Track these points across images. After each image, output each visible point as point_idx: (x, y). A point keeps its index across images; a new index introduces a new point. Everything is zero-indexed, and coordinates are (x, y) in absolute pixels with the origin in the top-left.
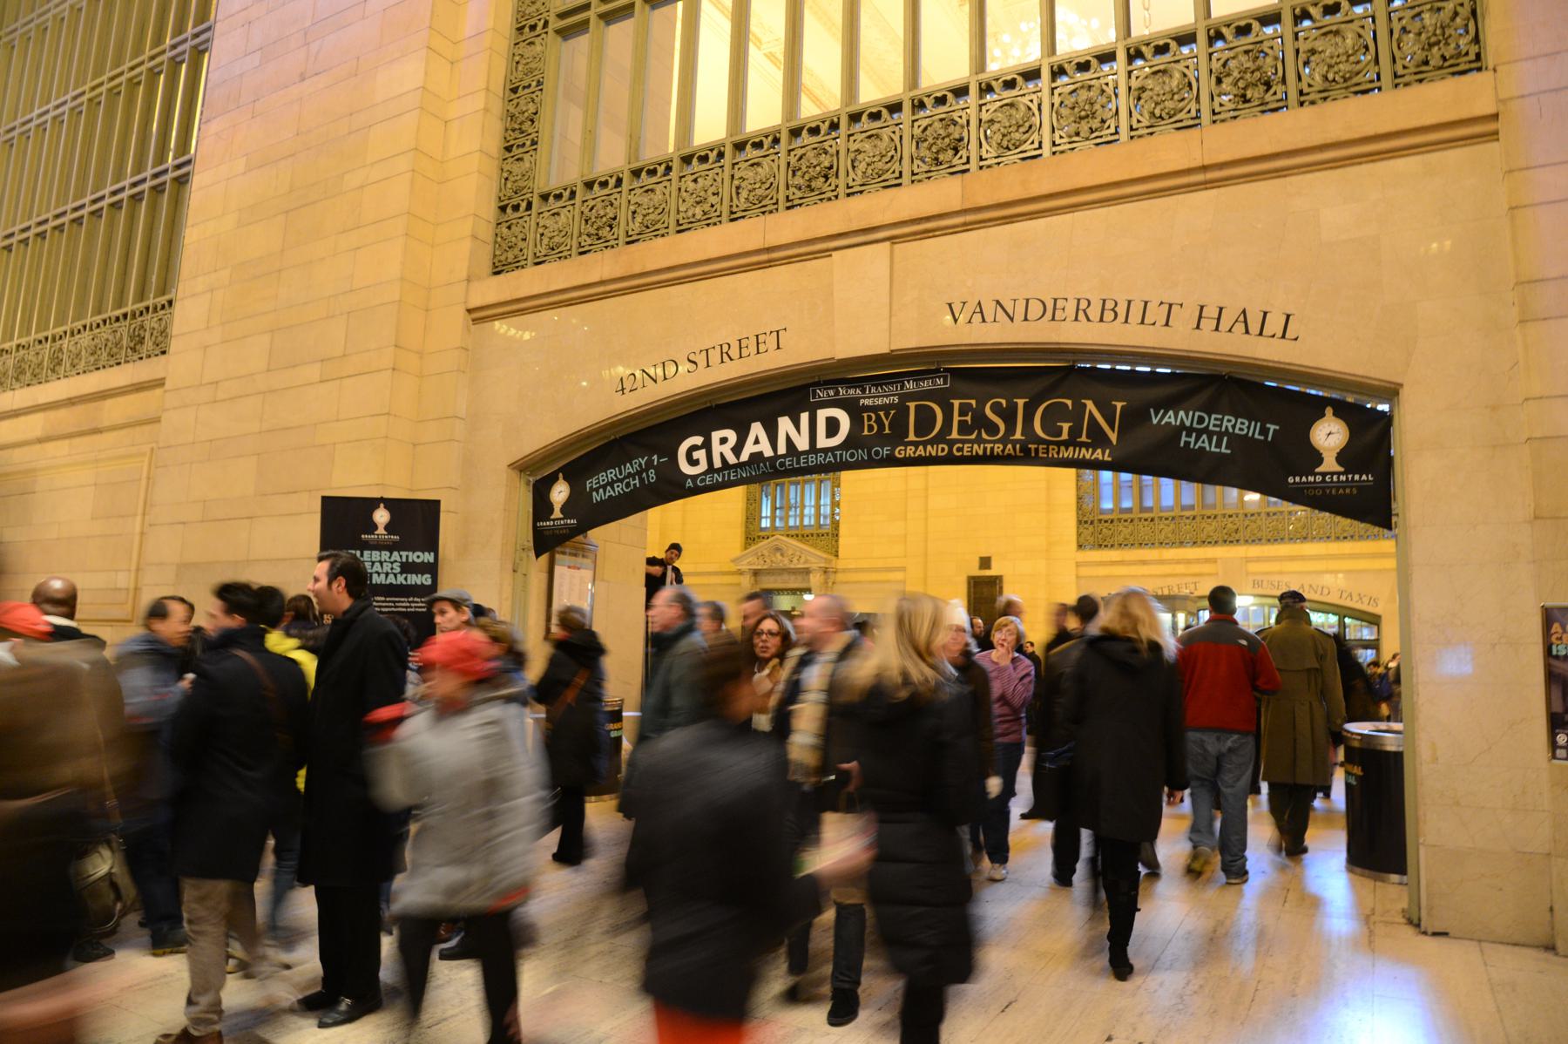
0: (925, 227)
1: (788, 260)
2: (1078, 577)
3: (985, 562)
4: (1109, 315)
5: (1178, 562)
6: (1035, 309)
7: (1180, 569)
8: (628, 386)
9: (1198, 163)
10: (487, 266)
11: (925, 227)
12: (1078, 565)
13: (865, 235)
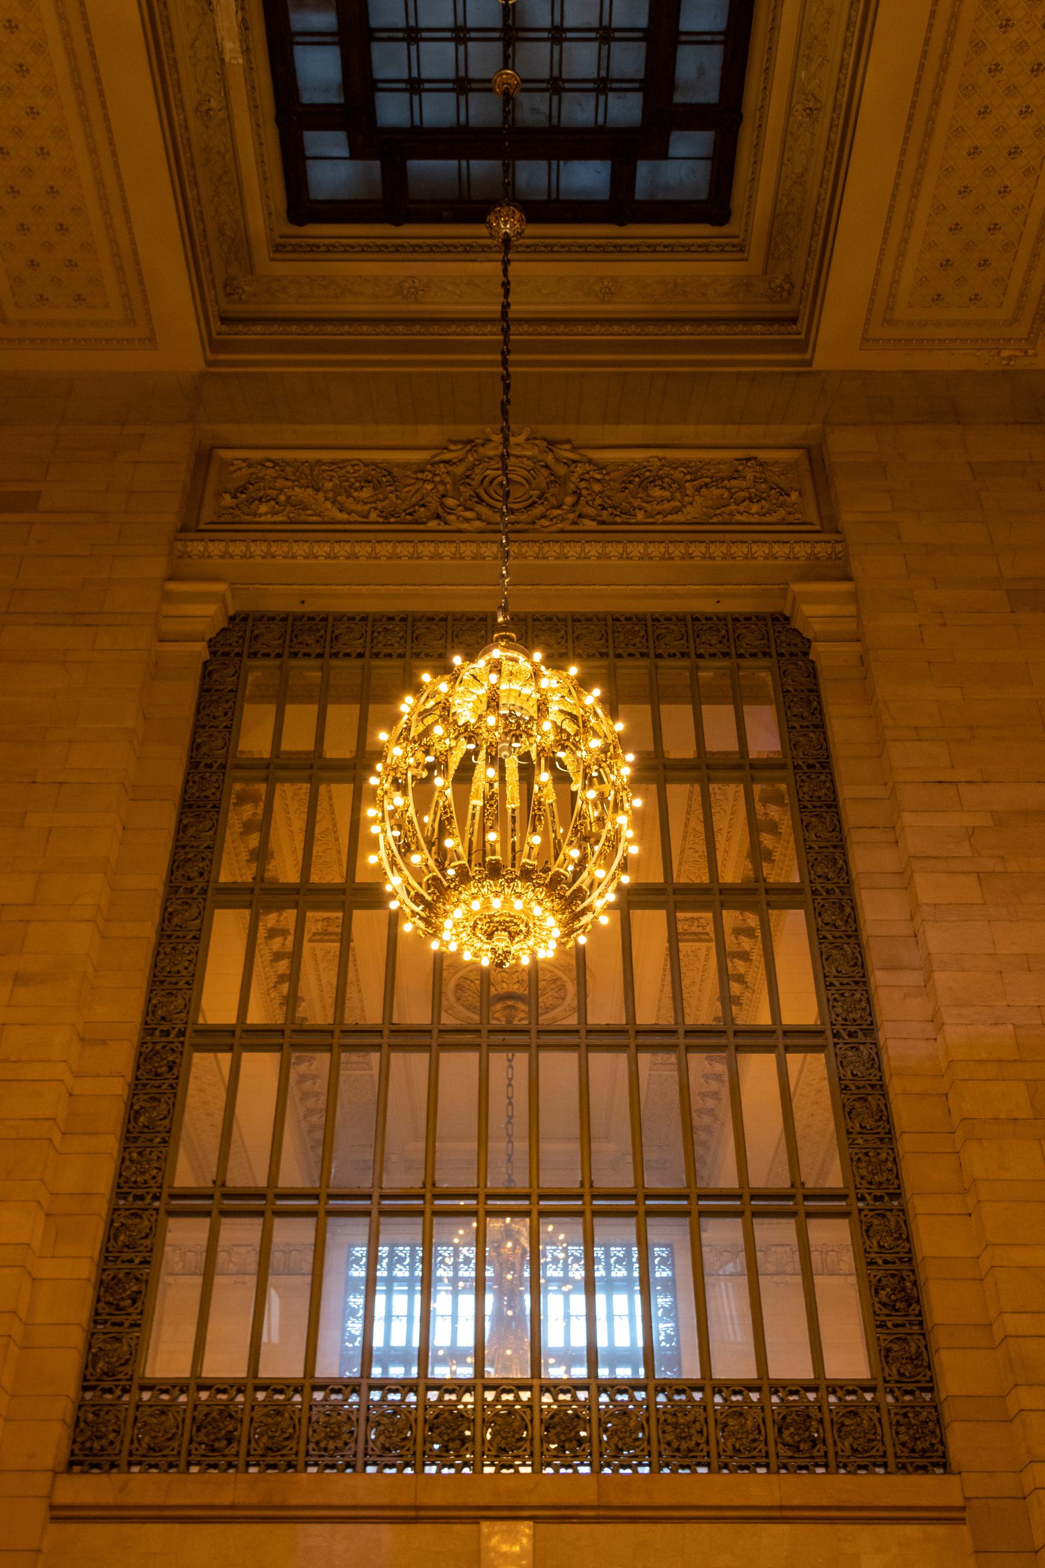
1: (435, 1520)
9: (777, 1503)
10: (64, 1456)
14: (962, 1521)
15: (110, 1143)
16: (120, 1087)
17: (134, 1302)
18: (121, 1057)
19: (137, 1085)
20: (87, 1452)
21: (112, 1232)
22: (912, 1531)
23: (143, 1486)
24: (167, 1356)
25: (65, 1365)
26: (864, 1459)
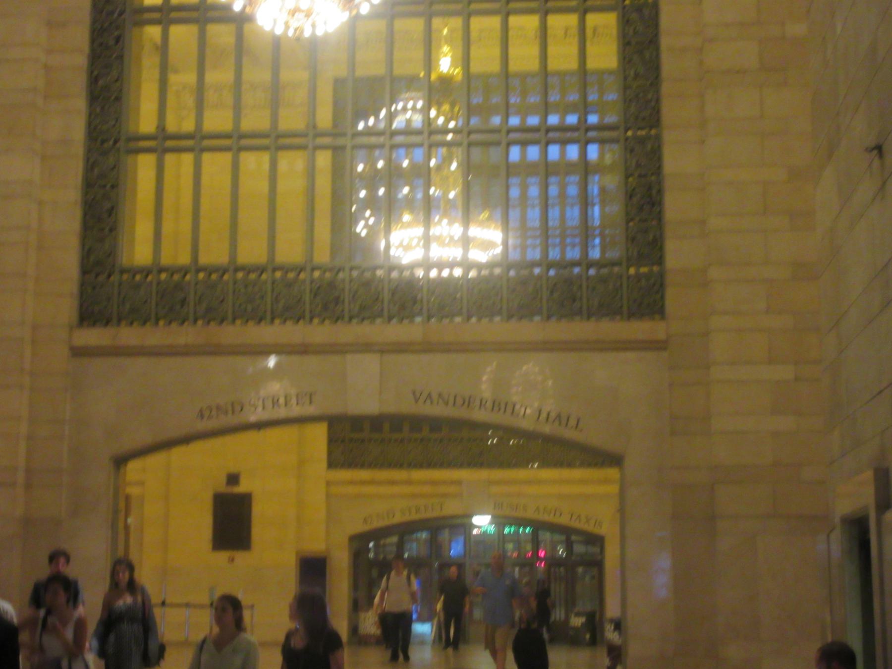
0: (401, 348)
2: (328, 495)
3: (233, 479)
4: (496, 408)
5: (426, 483)
6: (459, 401)
7: (427, 489)
8: (207, 414)
10: (75, 317)
11: (401, 348)
12: (328, 483)
13: (366, 347)
14: (665, 349)
15: (80, 104)
16: (81, 60)
17: (110, 215)
18: (79, 36)
19: (94, 57)
20: (88, 316)
21: (90, 166)
22: (631, 355)
23: (129, 335)
24: (138, 249)
25: (68, 260)
26: (608, 309)
